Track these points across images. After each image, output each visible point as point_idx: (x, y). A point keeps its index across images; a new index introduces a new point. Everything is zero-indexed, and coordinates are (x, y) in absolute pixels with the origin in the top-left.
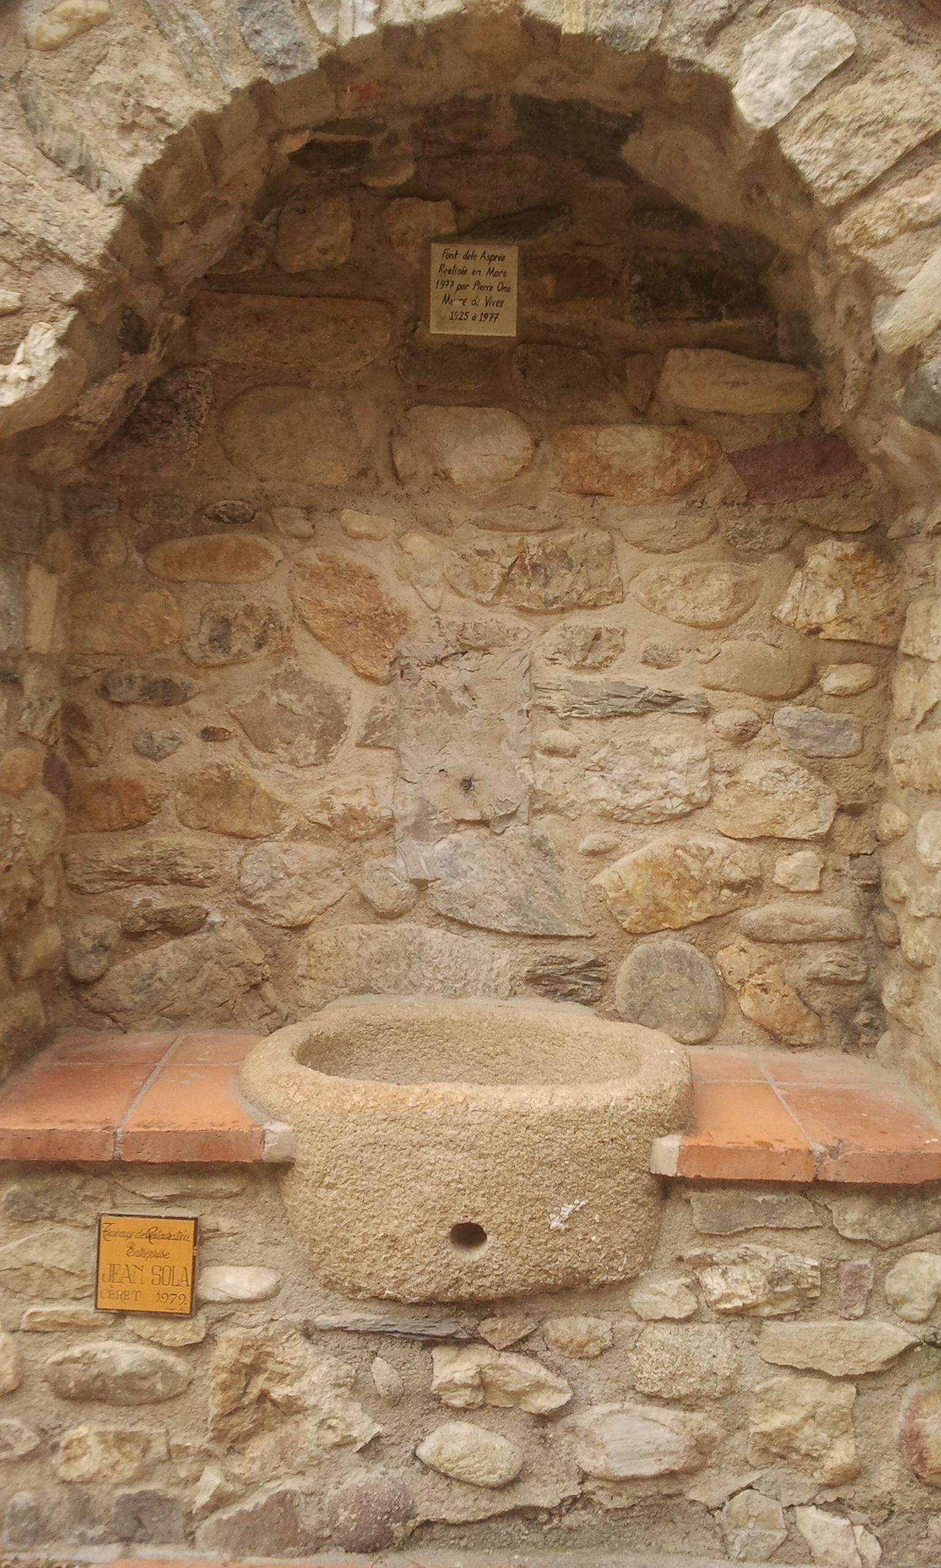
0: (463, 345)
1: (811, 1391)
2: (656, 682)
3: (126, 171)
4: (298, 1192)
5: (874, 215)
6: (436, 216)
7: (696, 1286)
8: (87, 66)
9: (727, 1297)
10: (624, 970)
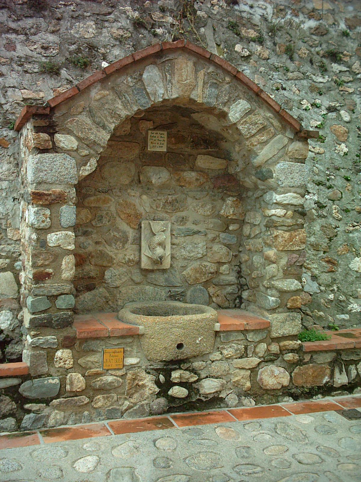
0: (155, 153)
1: (243, 372)
2: (195, 228)
3: (112, 126)
4: (145, 341)
6: (149, 125)
7: (221, 353)
8: (103, 105)
9: (228, 355)
10: (189, 293)
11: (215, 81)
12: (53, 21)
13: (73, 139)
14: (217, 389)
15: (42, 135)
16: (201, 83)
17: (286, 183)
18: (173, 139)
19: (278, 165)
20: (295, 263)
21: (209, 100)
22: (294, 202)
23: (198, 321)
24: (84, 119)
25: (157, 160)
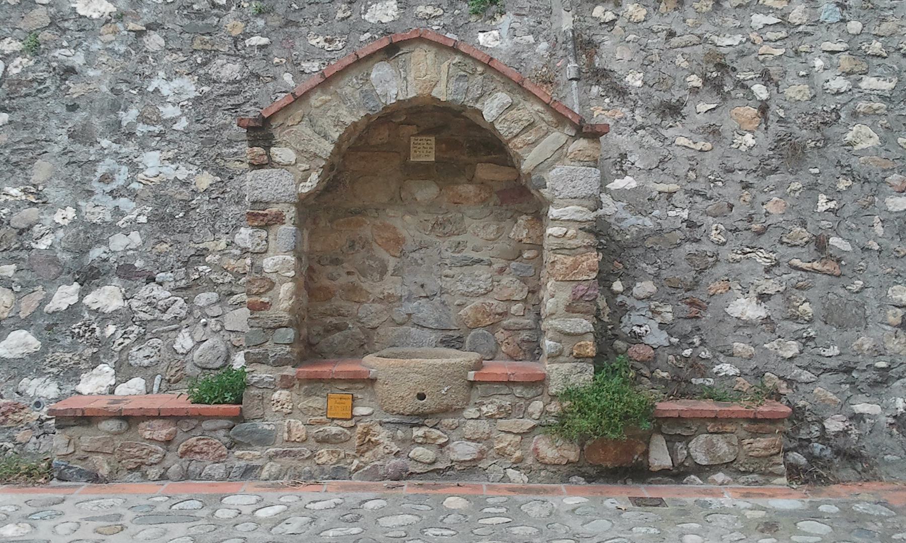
0: (419, 163)
1: (510, 437)
2: (476, 256)
3: (336, 136)
4: (379, 387)
5: (518, 141)
6: (412, 129)
7: (480, 410)
8: (325, 111)
9: (488, 412)
10: (468, 339)
11: (463, 73)
12: (343, 6)
13: (291, 151)
14: (474, 456)
15: (255, 149)
16: (444, 77)
17: (565, 193)
18: (444, 146)
19: (554, 171)
20: (581, 297)
21: (455, 97)
22: (578, 217)
23: (443, 365)
24: (306, 130)
25: (423, 172)
